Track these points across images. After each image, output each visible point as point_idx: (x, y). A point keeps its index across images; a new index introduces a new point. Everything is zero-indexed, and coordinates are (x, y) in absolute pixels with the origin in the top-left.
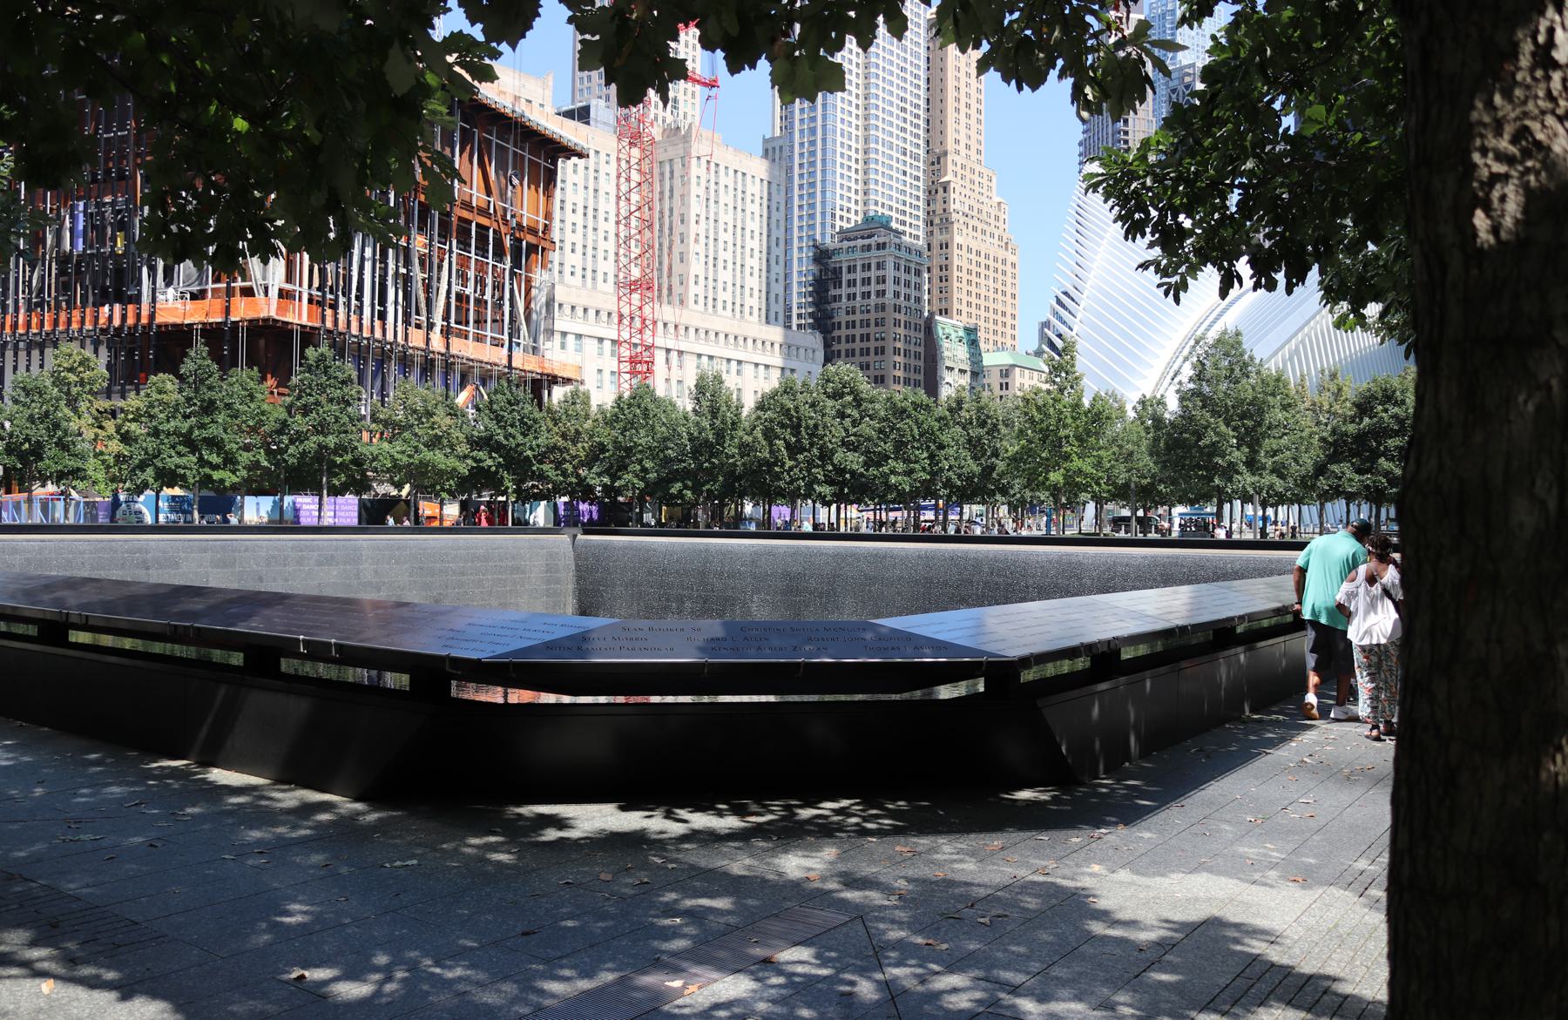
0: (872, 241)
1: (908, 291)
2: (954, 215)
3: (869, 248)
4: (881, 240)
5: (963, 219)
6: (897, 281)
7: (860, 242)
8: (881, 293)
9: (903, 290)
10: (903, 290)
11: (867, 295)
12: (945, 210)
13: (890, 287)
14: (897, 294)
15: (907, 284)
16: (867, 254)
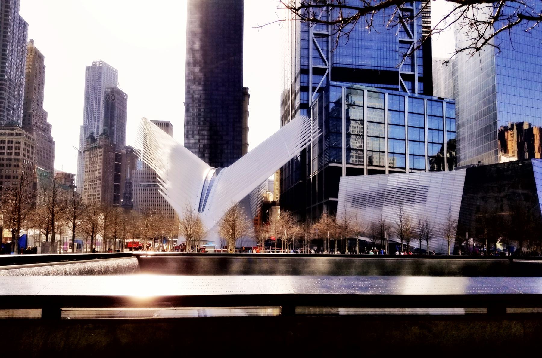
0: (14, 132)
1: (28, 154)
2: (33, 126)
3: (12, 134)
4: (19, 132)
5: (36, 128)
6: (25, 150)
7: (7, 131)
8: (18, 154)
9: (27, 154)
10: (27, 154)
11: (9, 154)
12: (29, 124)
13: (22, 152)
14: (24, 155)
15: (28, 152)
16: (11, 137)
